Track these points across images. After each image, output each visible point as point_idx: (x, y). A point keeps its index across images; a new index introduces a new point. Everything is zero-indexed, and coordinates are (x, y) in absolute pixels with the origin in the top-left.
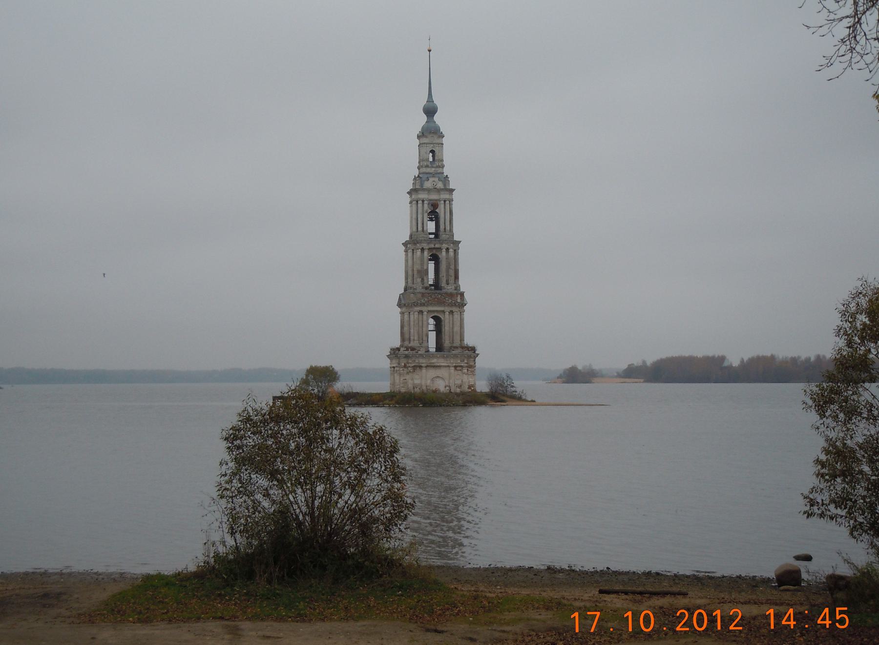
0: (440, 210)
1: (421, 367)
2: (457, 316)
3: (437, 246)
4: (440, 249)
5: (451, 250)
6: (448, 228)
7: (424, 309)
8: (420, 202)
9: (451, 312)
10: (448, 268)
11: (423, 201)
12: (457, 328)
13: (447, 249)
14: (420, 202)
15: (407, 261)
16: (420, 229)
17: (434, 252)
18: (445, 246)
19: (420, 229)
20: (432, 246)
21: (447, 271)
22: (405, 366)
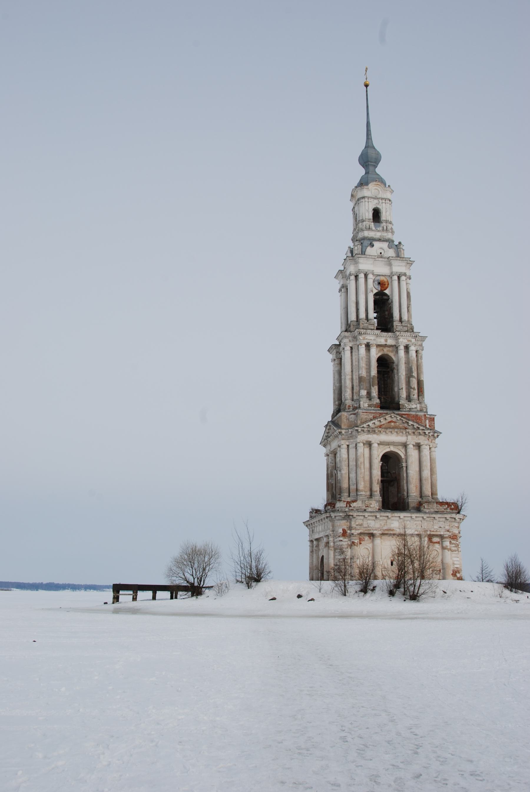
0: (393, 292)
1: (372, 535)
2: (426, 451)
3: (391, 342)
4: (396, 348)
5: (413, 349)
6: (405, 317)
7: (374, 438)
8: (362, 276)
9: (418, 446)
10: (409, 376)
11: (366, 276)
12: (426, 473)
13: (407, 348)
14: (362, 276)
15: (339, 373)
16: (362, 315)
17: (386, 351)
18: (403, 341)
19: (362, 315)
20: (382, 341)
21: (408, 383)
22: (344, 533)
